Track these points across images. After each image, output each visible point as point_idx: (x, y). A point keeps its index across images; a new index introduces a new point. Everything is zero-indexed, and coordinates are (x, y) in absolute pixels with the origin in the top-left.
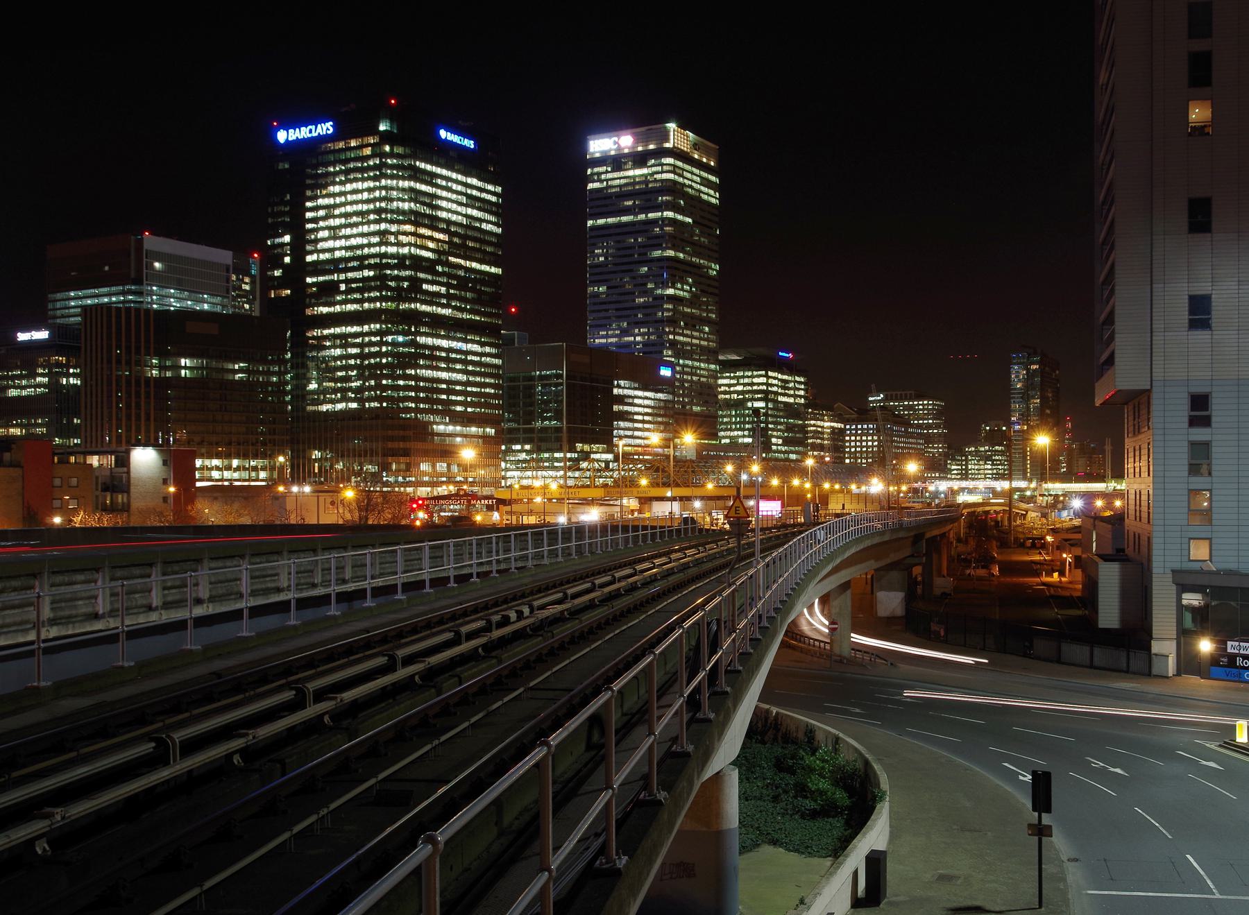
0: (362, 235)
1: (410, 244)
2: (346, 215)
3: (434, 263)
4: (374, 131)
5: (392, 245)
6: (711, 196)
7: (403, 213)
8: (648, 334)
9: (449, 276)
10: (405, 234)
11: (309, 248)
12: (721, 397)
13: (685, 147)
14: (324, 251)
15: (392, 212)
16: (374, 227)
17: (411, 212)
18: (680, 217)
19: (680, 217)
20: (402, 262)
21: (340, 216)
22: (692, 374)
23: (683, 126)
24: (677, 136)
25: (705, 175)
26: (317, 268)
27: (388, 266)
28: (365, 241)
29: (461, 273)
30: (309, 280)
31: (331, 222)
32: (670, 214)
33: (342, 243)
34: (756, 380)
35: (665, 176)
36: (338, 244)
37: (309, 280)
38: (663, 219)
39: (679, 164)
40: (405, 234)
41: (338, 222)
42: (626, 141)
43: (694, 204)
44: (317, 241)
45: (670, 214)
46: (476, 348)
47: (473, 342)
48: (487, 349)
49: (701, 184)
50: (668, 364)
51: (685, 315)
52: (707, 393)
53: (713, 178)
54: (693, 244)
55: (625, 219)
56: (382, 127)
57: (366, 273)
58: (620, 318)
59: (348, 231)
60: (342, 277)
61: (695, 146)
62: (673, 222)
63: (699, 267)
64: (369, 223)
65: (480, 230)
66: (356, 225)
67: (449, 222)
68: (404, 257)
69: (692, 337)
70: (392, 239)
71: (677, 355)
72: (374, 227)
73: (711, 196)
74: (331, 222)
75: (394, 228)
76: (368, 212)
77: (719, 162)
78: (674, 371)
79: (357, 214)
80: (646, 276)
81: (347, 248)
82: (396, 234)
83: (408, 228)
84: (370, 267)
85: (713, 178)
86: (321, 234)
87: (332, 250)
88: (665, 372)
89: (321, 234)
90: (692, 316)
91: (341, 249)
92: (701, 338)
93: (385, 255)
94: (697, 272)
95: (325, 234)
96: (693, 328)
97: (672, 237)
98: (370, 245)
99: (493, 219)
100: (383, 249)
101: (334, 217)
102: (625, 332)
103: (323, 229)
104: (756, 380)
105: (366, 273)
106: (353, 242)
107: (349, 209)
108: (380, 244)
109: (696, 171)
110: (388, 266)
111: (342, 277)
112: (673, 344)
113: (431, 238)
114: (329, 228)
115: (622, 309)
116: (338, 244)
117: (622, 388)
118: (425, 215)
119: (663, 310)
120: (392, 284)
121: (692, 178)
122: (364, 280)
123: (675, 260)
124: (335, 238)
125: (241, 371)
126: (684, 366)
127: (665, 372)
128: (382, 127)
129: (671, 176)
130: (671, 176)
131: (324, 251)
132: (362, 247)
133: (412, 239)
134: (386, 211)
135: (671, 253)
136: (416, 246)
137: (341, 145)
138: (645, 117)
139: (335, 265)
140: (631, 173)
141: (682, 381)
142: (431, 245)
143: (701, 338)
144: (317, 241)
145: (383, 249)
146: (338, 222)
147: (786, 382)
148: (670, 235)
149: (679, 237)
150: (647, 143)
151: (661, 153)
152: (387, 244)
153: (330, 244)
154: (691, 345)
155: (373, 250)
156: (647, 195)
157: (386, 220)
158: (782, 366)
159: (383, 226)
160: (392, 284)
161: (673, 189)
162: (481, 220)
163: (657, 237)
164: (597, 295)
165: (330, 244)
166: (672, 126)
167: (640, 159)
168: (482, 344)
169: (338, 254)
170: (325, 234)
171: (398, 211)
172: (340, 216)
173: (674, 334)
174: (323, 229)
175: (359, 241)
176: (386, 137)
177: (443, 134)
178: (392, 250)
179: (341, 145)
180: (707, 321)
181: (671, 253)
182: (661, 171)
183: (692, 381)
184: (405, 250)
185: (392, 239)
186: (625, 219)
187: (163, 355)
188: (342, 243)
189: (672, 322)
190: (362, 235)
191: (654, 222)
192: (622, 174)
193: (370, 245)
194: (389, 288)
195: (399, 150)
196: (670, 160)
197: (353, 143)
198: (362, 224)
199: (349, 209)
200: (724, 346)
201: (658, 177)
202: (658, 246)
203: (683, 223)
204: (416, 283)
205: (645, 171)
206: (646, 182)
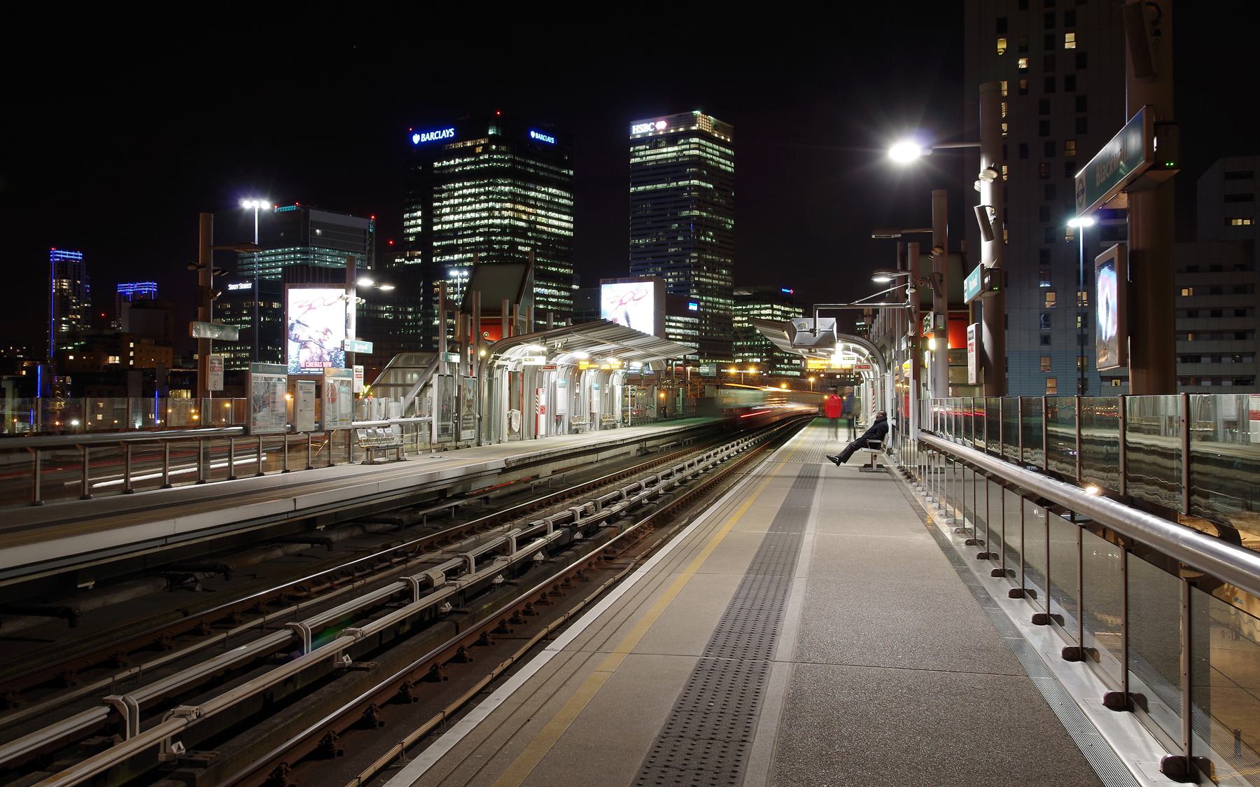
0: (475, 211)
1: (509, 217)
2: (464, 196)
3: (525, 230)
4: (485, 135)
5: (497, 218)
6: (728, 166)
7: (506, 194)
8: (678, 276)
9: (536, 239)
10: (507, 209)
11: (435, 220)
12: (735, 325)
14: (446, 223)
15: (497, 194)
16: (484, 205)
17: (511, 193)
18: (703, 184)
19: (703, 184)
20: (504, 230)
21: (459, 197)
22: (712, 308)
23: (706, 112)
24: (703, 121)
25: (723, 149)
26: (441, 235)
27: (494, 234)
28: (477, 215)
29: (545, 237)
30: (435, 244)
31: (452, 201)
32: (696, 182)
33: (460, 217)
34: (763, 312)
35: (692, 152)
36: (457, 217)
37: (435, 244)
38: (690, 186)
39: (703, 142)
40: (507, 209)
41: (457, 201)
43: (714, 173)
44: (442, 215)
45: (696, 182)
46: (555, 292)
47: (552, 288)
48: (563, 293)
49: (720, 158)
50: (695, 301)
51: (707, 261)
52: (724, 321)
53: (729, 152)
54: (713, 204)
55: (660, 186)
56: (491, 132)
57: (478, 239)
58: (656, 264)
59: (465, 208)
60: (460, 242)
61: (715, 127)
62: (698, 188)
63: (720, 222)
64: (480, 202)
65: (558, 204)
66: (470, 203)
67: (536, 199)
68: (506, 226)
69: (713, 278)
70: (497, 213)
71: (701, 294)
72: (484, 205)
73: (728, 166)
74: (452, 201)
75: (498, 206)
76: (480, 194)
78: (699, 306)
79: (471, 195)
80: (677, 231)
81: (463, 221)
82: (500, 210)
83: (508, 205)
84: (480, 234)
85: (729, 152)
86: (444, 211)
87: (453, 222)
88: (693, 307)
89: (444, 211)
90: (712, 261)
91: (459, 221)
92: (721, 278)
93: (492, 226)
95: (448, 210)
96: (713, 271)
98: (481, 218)
99: (568, 195)
100: (491, 221)
101: (455, 198)
103: (446, 206)
104: (763, 312)
105: (478, 239)
106: (468, 216)
107: (465, 191)
108: (488, 218)
109: (716, 147)
110: (494, 234)
111: (460, 242)
112: (698, 284)
113: (524, 212)
114: (450, 206)
116: (457, 217)
118: (520, 195)
119: (691, 258)
120: (496, 247)
121: (713, 153)
122: (476, 243)
123: (700, 217)
124: (455, 213)
125: (384, 312)
126: (706, 302)
127: (693, 307)
128: (491, 132)
129: (697, 152)
130: (697, 152)
131: (446, 223)
132: (475, 219)
133: (510, 213)
134: (492, 193)
135: (696, 213)
136: (514, 218)
137: (460, 145)
139: (454, 233)
140: (665, 150)
141: (705, 314)
142: (524, 217)
143: (721, 278)
144: (442, 215)
145: (491, 221)
146: (457, 201)
147: (789, 312)
148: (695, 198)
149: (703, 199)
150: (677, 126)
151: (689, 134)
152: (494, 217)
153: (451, 218)
154: (712, 284)
155: (483, 222)
157: (492, 200)
158: (784, 300)
159: (491, 204)
160: (496, 247)
161: (698, 162)
162: (559, 197)
163: (686, 200)
164: (638, 246)
165: (451, 218)
166: (697, 113)
167: (672, 140)
168: (559, 289)
169: (456, 225)
170: (448, 210)
171: (501, 193)
172: (459, 197)
173: (699, 276)
174: (446, 206)
175: (473, 215)
176: (493, 139)
177: (533, 134)
178: (498, 221)
179: (460, 145)
180: (726, 266)
181: (696, 213)
183: (712, 315)
184: (506, 221)
185: (497, 213)
186: (660, 186)
188: (460, 217)
189: (697, 267)
190: (475, 211)
191: (684, 188)
192: (658, 151)
193: (481, 218)
194: (495, 250)
195: (503, 148)
196: (696, 140)
197: (469, 144)
198: (475, 203)
199: (465, 191)
200: (738, 284)
201: (686, 153)
202: (687, 208)
203: (706, 189)
204: (513, 246)
205: (676, 148)
206: (677, 158)
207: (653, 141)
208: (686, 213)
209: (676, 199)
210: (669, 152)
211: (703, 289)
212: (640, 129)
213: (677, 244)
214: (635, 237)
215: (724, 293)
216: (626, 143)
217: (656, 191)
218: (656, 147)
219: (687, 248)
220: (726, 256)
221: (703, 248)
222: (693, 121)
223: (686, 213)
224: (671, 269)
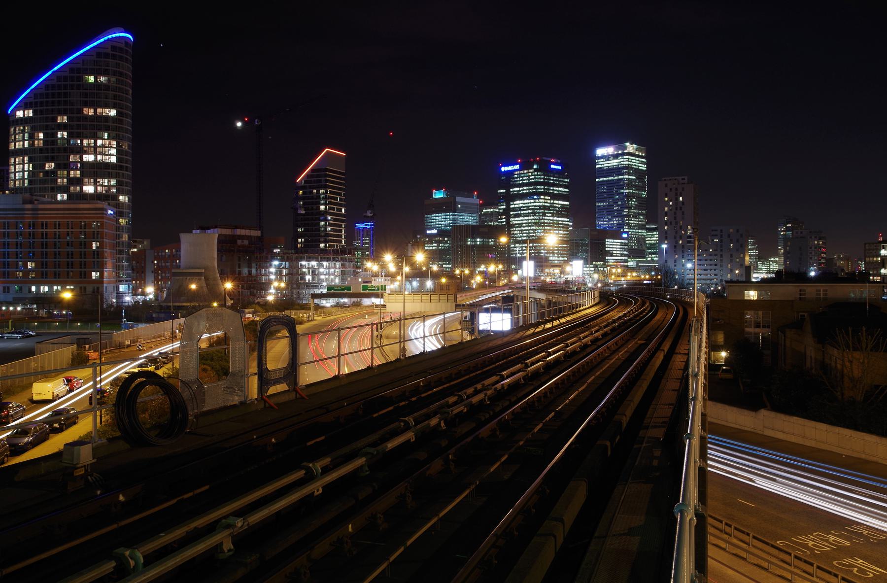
6: (644, 167)
13: (632, 151)
23: (631, 144)
24: (631, 148)
42: (610, 150)
43: (637, 172)
52: (641, 240)
58: (608, 215)
61: (637, 150)
73: (644, 167)
77: (646, 154)
88: (625, 235)
94: (639, 198)
97: (628, 185)
102: (610, 220)
112: (628, 224)
115: (609, 211)
117: (609, 242)
138: (618, 140)
150: (618, 150)
151: (623, 154)
156: (617, 170)
161: (628, 167)
166: (628, 144)
167: (616, 156)
180: (642, 214)
182: (624, 161)
187: (473, 238)
189: (628, 216)
200: (648, 223)
202: (623, 188)
207: (607, 158)
208: (622, 191)
209: (619, 184)
210: (614, 162)
211: (631, 227)
212: (600, 152)
213: (618, 205)
214: (599, 202)
215: (642, 227)
216: (593, 159)
217: (608, 181)
218: (608, 160)
219: (623, 207)
220: (642, 210)
221: (629, 208)
222: (625, 148)
223: (622, 191)
224: (615, 217)
